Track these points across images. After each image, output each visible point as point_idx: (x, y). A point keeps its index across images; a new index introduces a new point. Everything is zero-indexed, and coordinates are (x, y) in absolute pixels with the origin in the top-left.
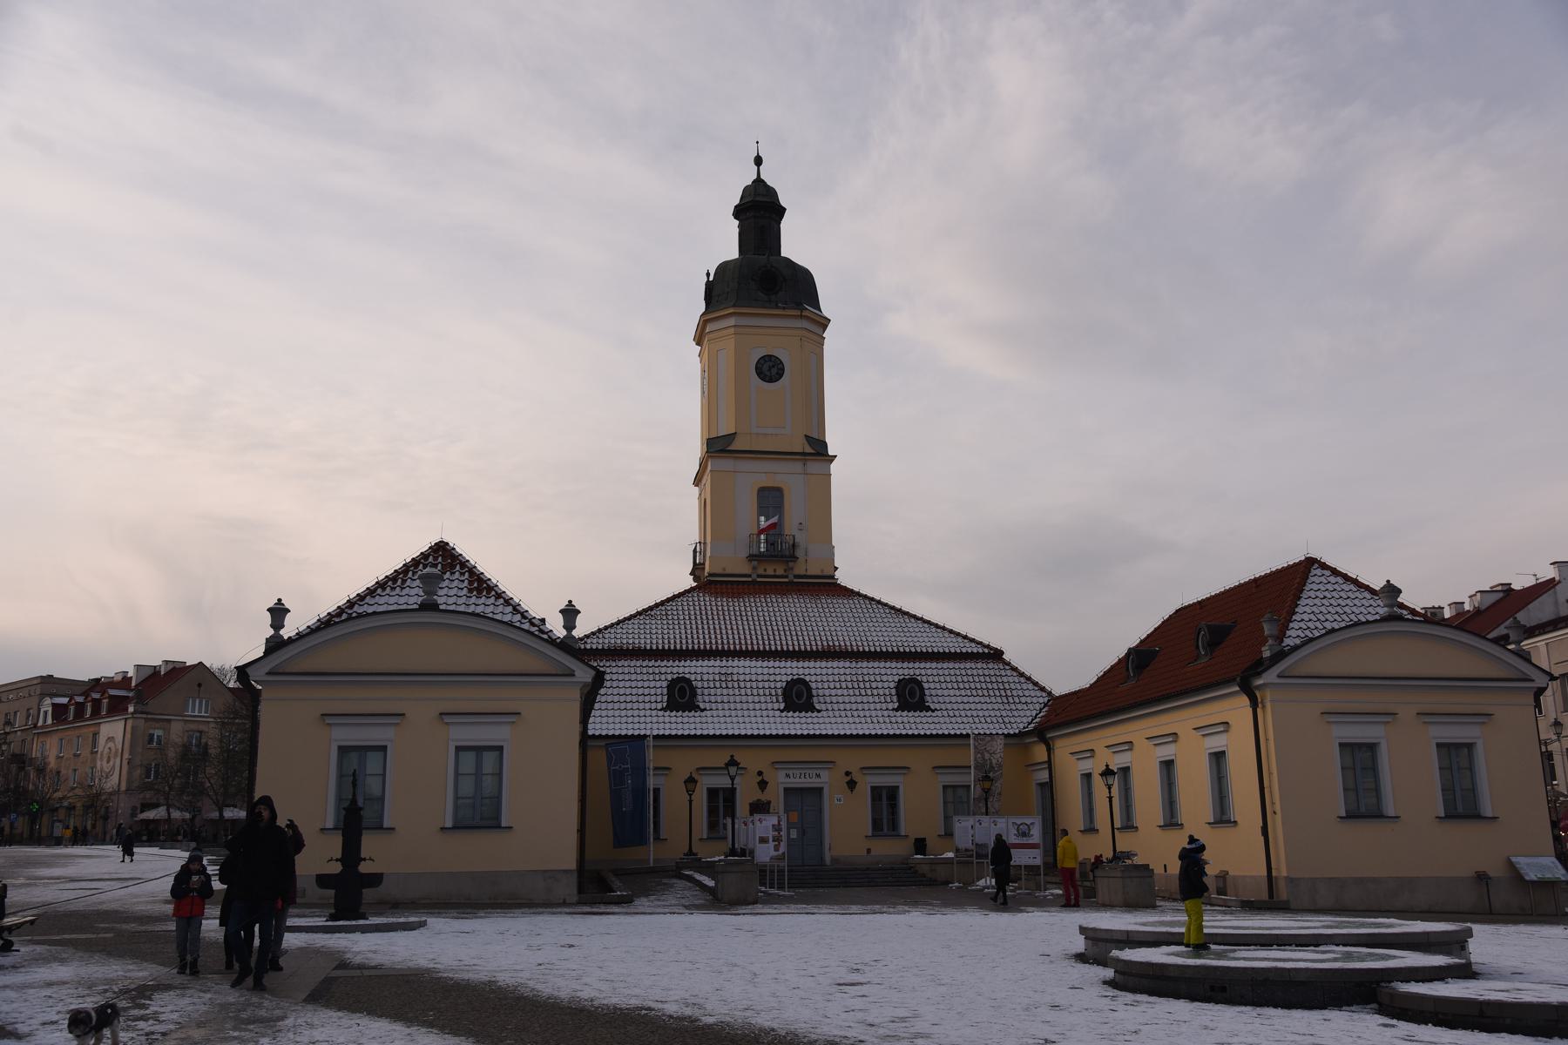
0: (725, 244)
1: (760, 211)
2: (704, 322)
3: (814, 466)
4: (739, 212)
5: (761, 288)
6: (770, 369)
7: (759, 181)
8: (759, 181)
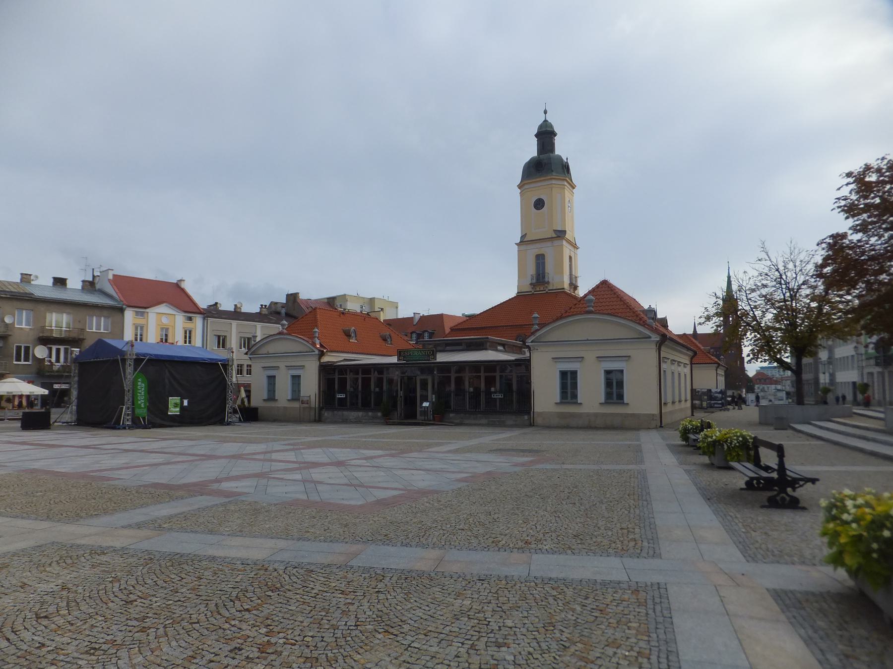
0: (531, 151)
1: (546, 136)
2: (520, 187)
3: (557, 243)
4: (536, 136)
5: (546, 166)
6: (539, 204)
7: (546, 121)
8: (546, 121)
